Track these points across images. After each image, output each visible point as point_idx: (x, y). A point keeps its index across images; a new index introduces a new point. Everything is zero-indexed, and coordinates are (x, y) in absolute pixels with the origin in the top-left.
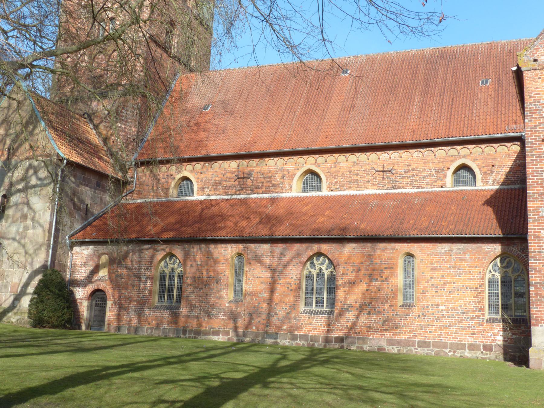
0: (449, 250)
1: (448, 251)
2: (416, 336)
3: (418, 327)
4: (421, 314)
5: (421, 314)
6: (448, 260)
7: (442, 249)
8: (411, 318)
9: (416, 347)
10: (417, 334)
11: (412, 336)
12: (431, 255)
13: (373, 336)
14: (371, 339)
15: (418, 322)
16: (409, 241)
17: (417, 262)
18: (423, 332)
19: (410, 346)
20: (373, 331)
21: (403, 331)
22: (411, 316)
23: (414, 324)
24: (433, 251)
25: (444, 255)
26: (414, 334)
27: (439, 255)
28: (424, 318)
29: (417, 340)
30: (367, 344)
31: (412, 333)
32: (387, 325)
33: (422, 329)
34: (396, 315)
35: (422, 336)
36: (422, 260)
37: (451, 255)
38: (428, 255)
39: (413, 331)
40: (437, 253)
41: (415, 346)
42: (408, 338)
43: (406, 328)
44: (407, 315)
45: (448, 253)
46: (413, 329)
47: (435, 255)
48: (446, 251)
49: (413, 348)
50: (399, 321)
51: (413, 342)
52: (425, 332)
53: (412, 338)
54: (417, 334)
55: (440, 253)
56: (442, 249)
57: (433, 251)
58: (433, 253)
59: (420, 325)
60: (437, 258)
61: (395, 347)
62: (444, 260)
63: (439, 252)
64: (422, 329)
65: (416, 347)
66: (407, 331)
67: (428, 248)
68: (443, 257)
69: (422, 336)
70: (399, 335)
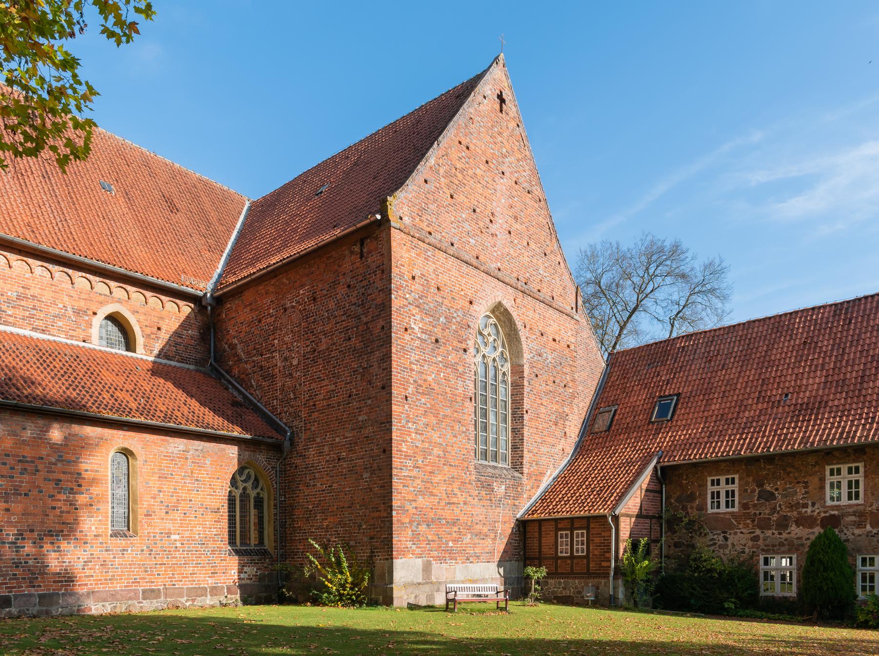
0: (184, 449)
1: (183, 451)
2: (139, 582)
3: (140, 568)
4: (145, 548)
5: (145, 548)
6: (182, 465)
7: (175, 447)
8: (130, 554)
10: (140, 578)
12: (160, 455)
15: (141, 560)
16: (125, 428)
17: (138, 464)
18: (148, 575)
19: (130, 599)
21: (117, 575)
22: (129, 552)
23: (135, 564)
24: (162, 449)
25: (177, 457)
27: (170, 456)
28: (150, 554)
32: (90, 569)
33: (146, 571)
34: (107, 551)
35: (147, 582)
36: (146, 461)
37: (187, 458)
38: (155, 455)
39: (133, 575)
40: (167, 452)
42: (125, 586)
43: (122, 572)
44: (124, 550)
45: (183, 454)
46: (134, 571)
47: (165, 456)
48: (180, 451)
49: (135, 602)
50: (110, 561)
51: (136, 592)
52: (151, 575)
53: (132, 586)
54: (140, 578)
55: (172, 453)
56: (175, 447)
57: (162, 449)
58: (162, 452)
59: (143, 565)
60: (167, 460)
61: (107, 604)
62: (177, 464)
63: (170, 451)
64: (146, 571)
65: (141, 600)
66: (124, 575)
67: (155, 443)
68: (176, 461)
69: (147, 582)
70: (112, 583)
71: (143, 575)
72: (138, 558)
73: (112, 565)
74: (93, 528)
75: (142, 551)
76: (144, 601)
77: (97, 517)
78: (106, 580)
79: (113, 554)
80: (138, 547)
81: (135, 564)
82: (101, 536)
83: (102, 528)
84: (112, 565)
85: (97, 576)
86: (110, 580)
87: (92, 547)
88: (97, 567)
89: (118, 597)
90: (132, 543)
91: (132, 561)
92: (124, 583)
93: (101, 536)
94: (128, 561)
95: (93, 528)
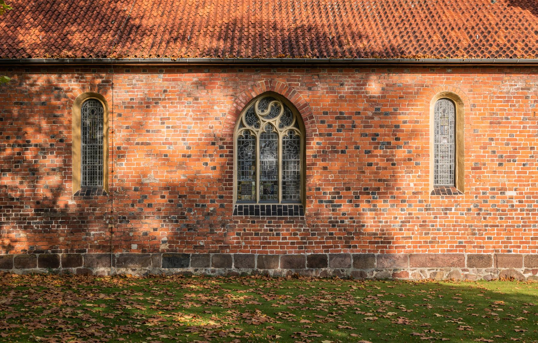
0: (524, 86)
1: (522, 89)
2: (465, 247)
3: (467, 230)
4: (472, 207)
5: (472, 207)
6: (521, 106)
7: (511, 85)
8: (454, 214)
9: (466, 267)
10: (466, 242)
11: (457, 247)
12: (491, 97)
13: (382, 252)
14: (378, 256)
15: (467, 221)
16: (449, 70)
17: (465, 109)
18: (476, 238)
19: (453, 265)
20: (382, 242)
21: (439, 238)
22: (453, 211)
23: (460, 226)
24: (494, 89)
25: (514, 97)
26: (460, 242)
27: (505, 97)
28: (479, 214)
29: (466, 254)
30: (373, 266)
31: (455, 242)
32: (409, 230)
33: (474, 234)
34: (427, 210)
35: (474, 247)
36: (474, 106)
37: (527, 97)
38: (486, 97)
39: (458, 238)
40: (501, 93)
41: (464, 266)
42: (448, 251)
43: (444, 234)
44: (447, 209)
45: (522, 93)
47: (498, 97)
48: (518, 89)
49: (459, 269)
50: (431, 222)
51: (460, 257)
52: (480, 239)
53: (456, 251)
54: (466, 242)
55: (508, 93)
56: (511, 85)
57: (494, 89)
58: (494, 93)
59: (469, 226)
60: (501, 102)
61: (426, 269)
62: (514, 106)
63: (505, 90)
64: (474, 234)
65: (466, 267)
66: (447, 238)
67: (485, 83)
68: (513, 101)
69: (474, 247)
70: (432, 247)
71: (468, 238)
72: (463, 218)
73: (433, 226)
74: (412, 185)
75: (469, 210)
76: (470, 269)
77: (416, 172)
78: (426, 242)
79: (433, 214)
80: (463, 206)
81: (460, 226)
82: (420, 193)
83: (421, 185)
84: (433, 226)
85: (416, 238)
86: (430, 242)
87: (410, 206)
88: (416, 228)
89: (439, 262)
90: (456, 201)
91: (456, 222)
92: (447, 246)
93: (420, 193)
94: (453, 222)
95: (412, 185)
